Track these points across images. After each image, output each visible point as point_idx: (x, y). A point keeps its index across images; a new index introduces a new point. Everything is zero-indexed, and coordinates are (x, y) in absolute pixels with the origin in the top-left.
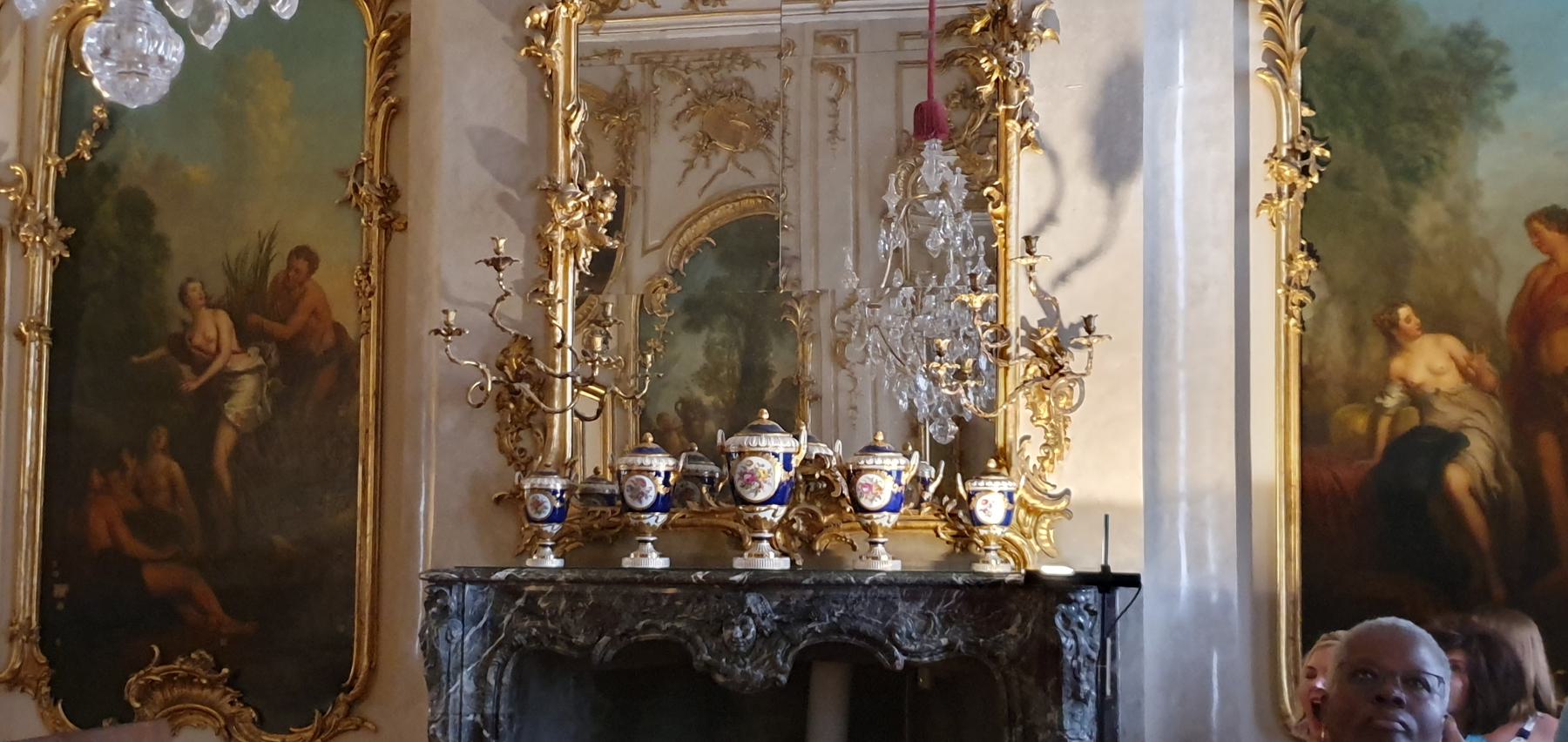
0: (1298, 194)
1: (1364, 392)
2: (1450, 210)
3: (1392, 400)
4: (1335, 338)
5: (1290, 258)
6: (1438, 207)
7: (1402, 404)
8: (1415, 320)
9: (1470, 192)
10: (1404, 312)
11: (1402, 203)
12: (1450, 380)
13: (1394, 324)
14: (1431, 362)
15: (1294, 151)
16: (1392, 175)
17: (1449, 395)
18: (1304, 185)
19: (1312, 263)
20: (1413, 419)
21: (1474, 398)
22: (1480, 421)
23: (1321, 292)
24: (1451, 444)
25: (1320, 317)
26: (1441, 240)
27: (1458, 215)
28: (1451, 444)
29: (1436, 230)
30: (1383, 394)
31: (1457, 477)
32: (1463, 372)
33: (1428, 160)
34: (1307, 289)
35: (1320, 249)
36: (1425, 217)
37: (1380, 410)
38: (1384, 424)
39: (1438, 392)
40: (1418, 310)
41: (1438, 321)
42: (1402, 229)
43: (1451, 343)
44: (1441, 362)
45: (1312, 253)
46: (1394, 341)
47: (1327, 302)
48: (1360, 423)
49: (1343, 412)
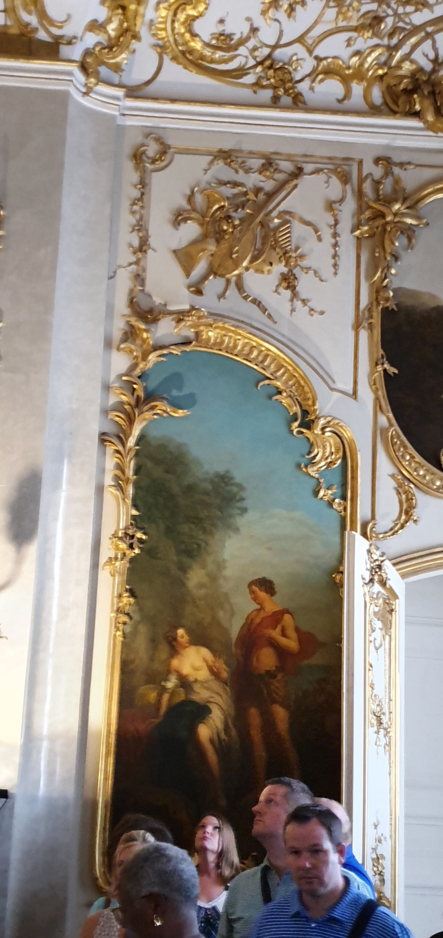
0: (127, 559)
1: (156, 678)
2: (209, 575)
3: (171, 683)
4: (141, 644)
5: (120, 596)
6: (202, 572)
7: (176, 686)
8: (186, 638)
9: (220, 566)
10: (181, 632)
11: (184, 569)
12: (204, 674)
13: (175, 639)
14: (194, 662)
15: (126, 534)
16: (179, 552)
17: (202, 682)
18: (131, 554)
19: (132, 600)
20: (181, 696)
21: (216, 686)
22: (218, 699)
23: (136, 617)
24: (201, 711)
25: (135, 632)
26: (203, 592)
27: (213, 578)
28: (201, 711)
29: (201, 586)
30: (166, 680)
31: (204, 732)
32: (211, 669)
33: (199, 546)
34: (128, 614)
35: (138, 593)
36: (195, 577)
37: (164, 689)
38: (166, 697)
39: (196, 681)
40: (189, 632)
41: (199, 639)
42: (183, 584)
43: (205, 652)
44: (199, 663)
45: (132, 593)
46: (174, 648)
47: (138, 623)
48: (153, 696)
49: (142, 689)
